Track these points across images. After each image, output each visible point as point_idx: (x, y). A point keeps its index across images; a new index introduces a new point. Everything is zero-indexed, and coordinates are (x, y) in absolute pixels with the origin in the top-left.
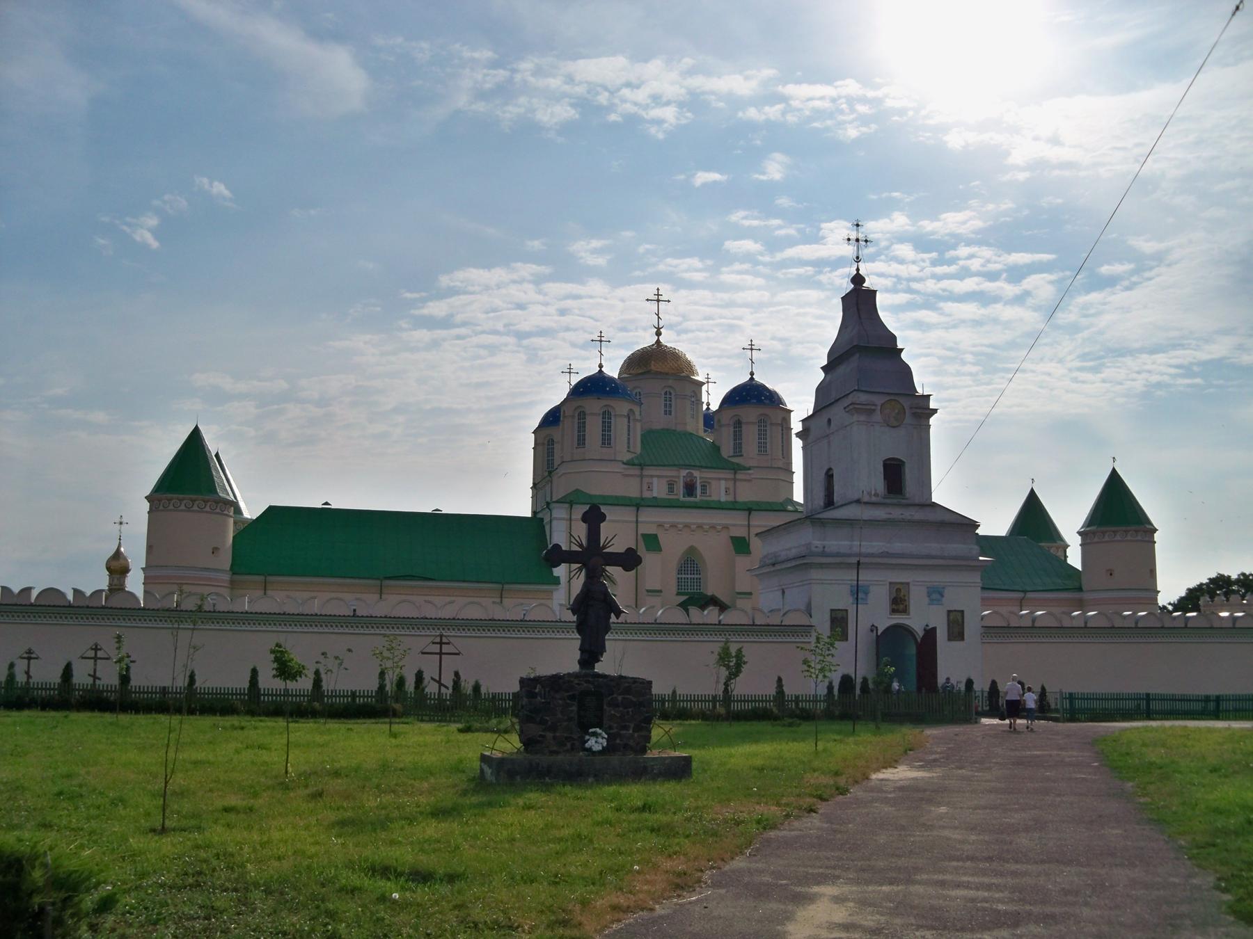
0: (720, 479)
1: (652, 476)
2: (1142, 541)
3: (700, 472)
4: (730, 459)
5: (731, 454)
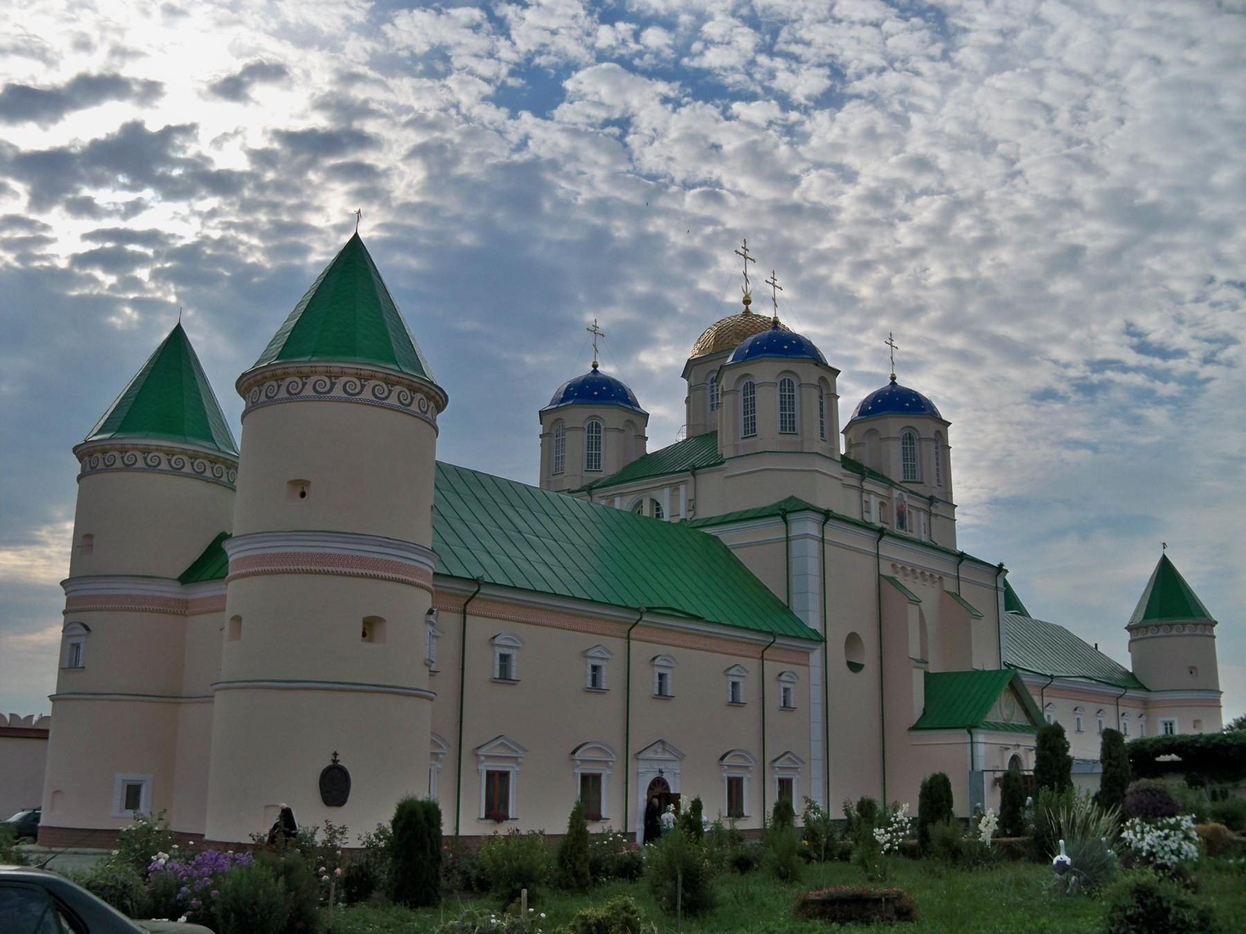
0: (918, 509)
1: (869, 492)
2: (1166, 636)
3: (908, 497)
4: (902, 484)
5: (901, 480)
